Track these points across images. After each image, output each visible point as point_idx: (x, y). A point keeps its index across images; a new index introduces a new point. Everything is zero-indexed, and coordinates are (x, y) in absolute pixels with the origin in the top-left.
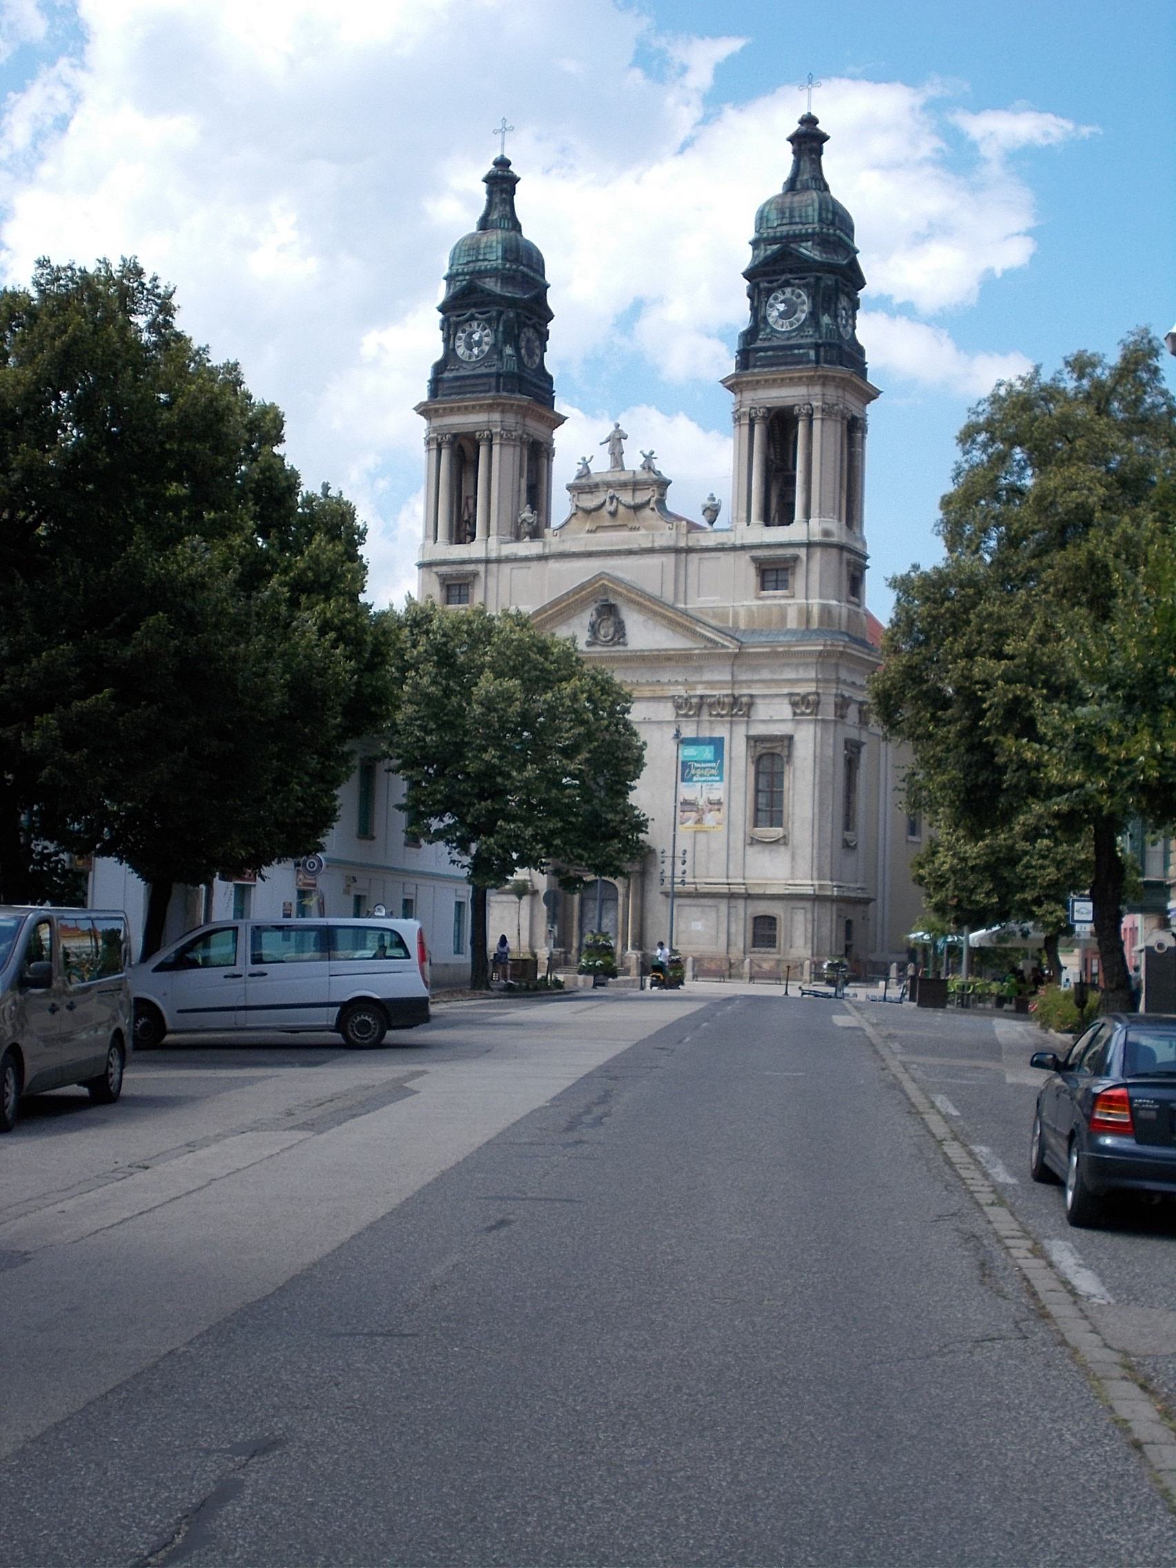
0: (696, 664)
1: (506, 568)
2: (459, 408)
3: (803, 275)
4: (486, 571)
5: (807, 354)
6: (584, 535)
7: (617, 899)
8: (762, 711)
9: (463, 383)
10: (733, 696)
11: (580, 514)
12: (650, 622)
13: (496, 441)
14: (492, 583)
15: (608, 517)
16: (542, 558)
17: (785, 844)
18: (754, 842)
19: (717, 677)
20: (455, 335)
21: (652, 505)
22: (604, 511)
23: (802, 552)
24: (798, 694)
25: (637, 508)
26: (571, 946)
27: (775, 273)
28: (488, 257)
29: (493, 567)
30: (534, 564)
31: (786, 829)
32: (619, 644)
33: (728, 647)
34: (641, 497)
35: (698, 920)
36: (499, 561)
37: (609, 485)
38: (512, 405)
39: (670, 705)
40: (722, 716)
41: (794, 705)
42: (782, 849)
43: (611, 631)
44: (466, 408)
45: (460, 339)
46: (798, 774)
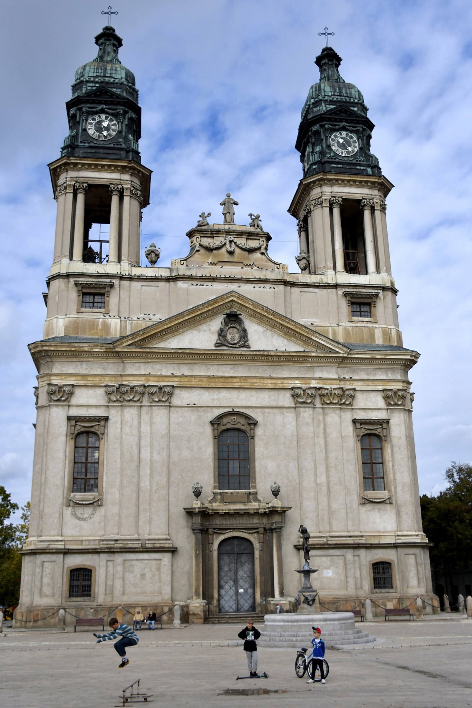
0: (309, 365)
1: (136, 285)
2: (96, 165)
3: (355, 125)
4: (120, 285)
5: (366, 170)
6: (206, 265)
7: (252, 554)
8: (361, 401)
9: (97, 151)
10: (342, 389)
11: (202, 251)
12: (269, 333)
13: (126, 193)
14: (124, 295)
15: (227, 255)
16: (168, 280)
17: (391, 503)
18: (366, 501)
19: (325, 375)
20: (87, 121)
21: (263, 250)
22: (223, 250)
23: (381, 292)
24: (391, 390)
25: (251, 251)
26: (212, 598)
27: (336, 120)
28: (113, 75)
29: (125, 283)
30: (162, 284)
31: (389, 491)
32: (244, 346)
33: (340, 353)
34: (253, 244)
35: (328, 568)
36: (131, 278)
37: (228, 232)
38: (139, 171)
39: (288, 394)
40: (334, 404)
41: (386, 398)
42: (388, 507)
43: (237, 337)
44: (103, 166)
45: (91, 124)
46: (396, 449)
